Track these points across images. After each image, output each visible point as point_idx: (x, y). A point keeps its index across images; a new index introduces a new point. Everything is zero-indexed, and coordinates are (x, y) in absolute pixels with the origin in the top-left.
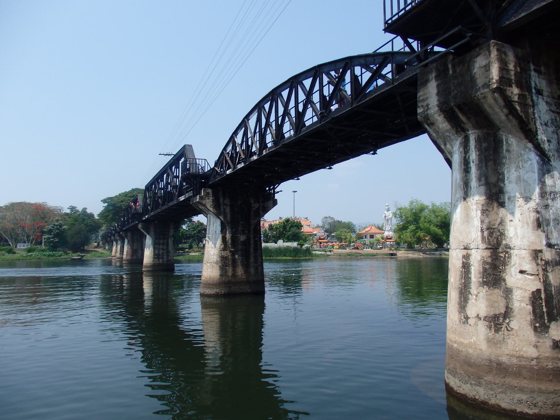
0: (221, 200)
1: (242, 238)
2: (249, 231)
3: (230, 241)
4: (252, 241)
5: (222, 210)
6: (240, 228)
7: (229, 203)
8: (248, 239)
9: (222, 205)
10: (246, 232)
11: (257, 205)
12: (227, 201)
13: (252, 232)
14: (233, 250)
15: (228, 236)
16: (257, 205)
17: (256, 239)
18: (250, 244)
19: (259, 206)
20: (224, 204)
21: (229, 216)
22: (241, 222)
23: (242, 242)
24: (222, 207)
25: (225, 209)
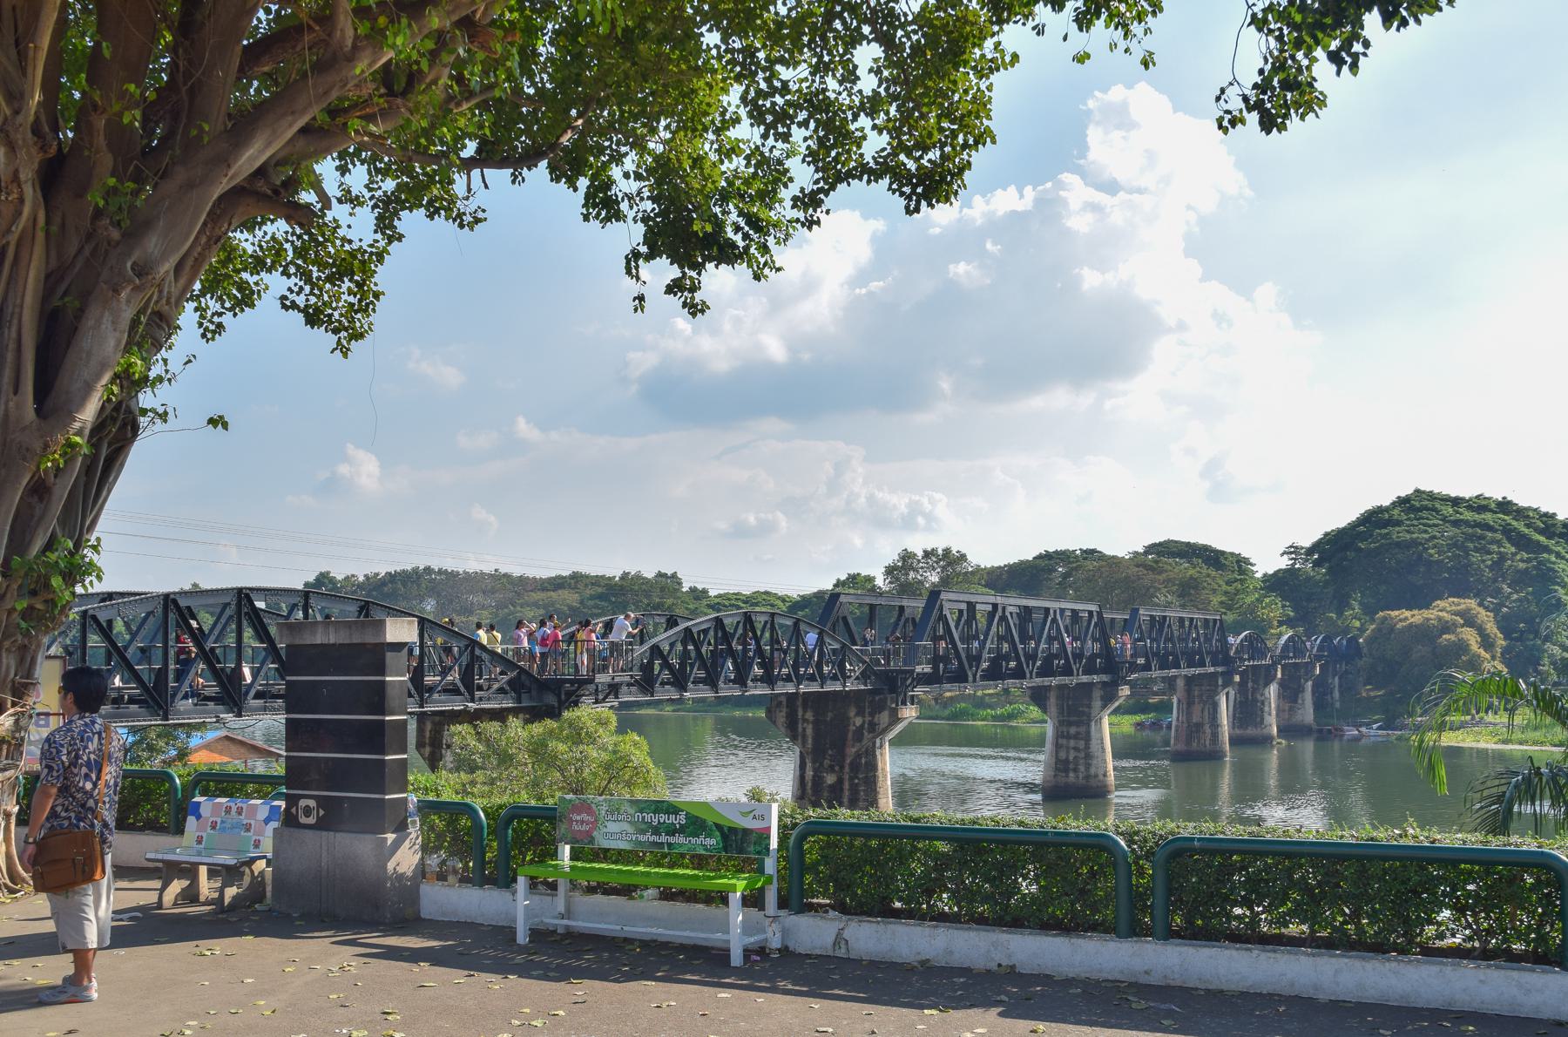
0: (800, 713)
1: (830, 779)
2: (842, 767)
3: (810, 784)
4: (846, 786)
5: (800, 729)
6: (827, 762)
7: (811, 718)
8: (840, 781)
9: (800, 721)
10: (837, 768)
11: (858, 721)
12: (809, 715)
13: (847, 769)
14: (813, 798)
15: (809, 773)
16: (858, 721)
17: (856, 781)
18: (842, 790)
19: (864, 722)
20: (805, 720)
21: (810, 741)
22: (830, 752)
23: (830, 786)
24: (800, 725)
25: (804, 729)
